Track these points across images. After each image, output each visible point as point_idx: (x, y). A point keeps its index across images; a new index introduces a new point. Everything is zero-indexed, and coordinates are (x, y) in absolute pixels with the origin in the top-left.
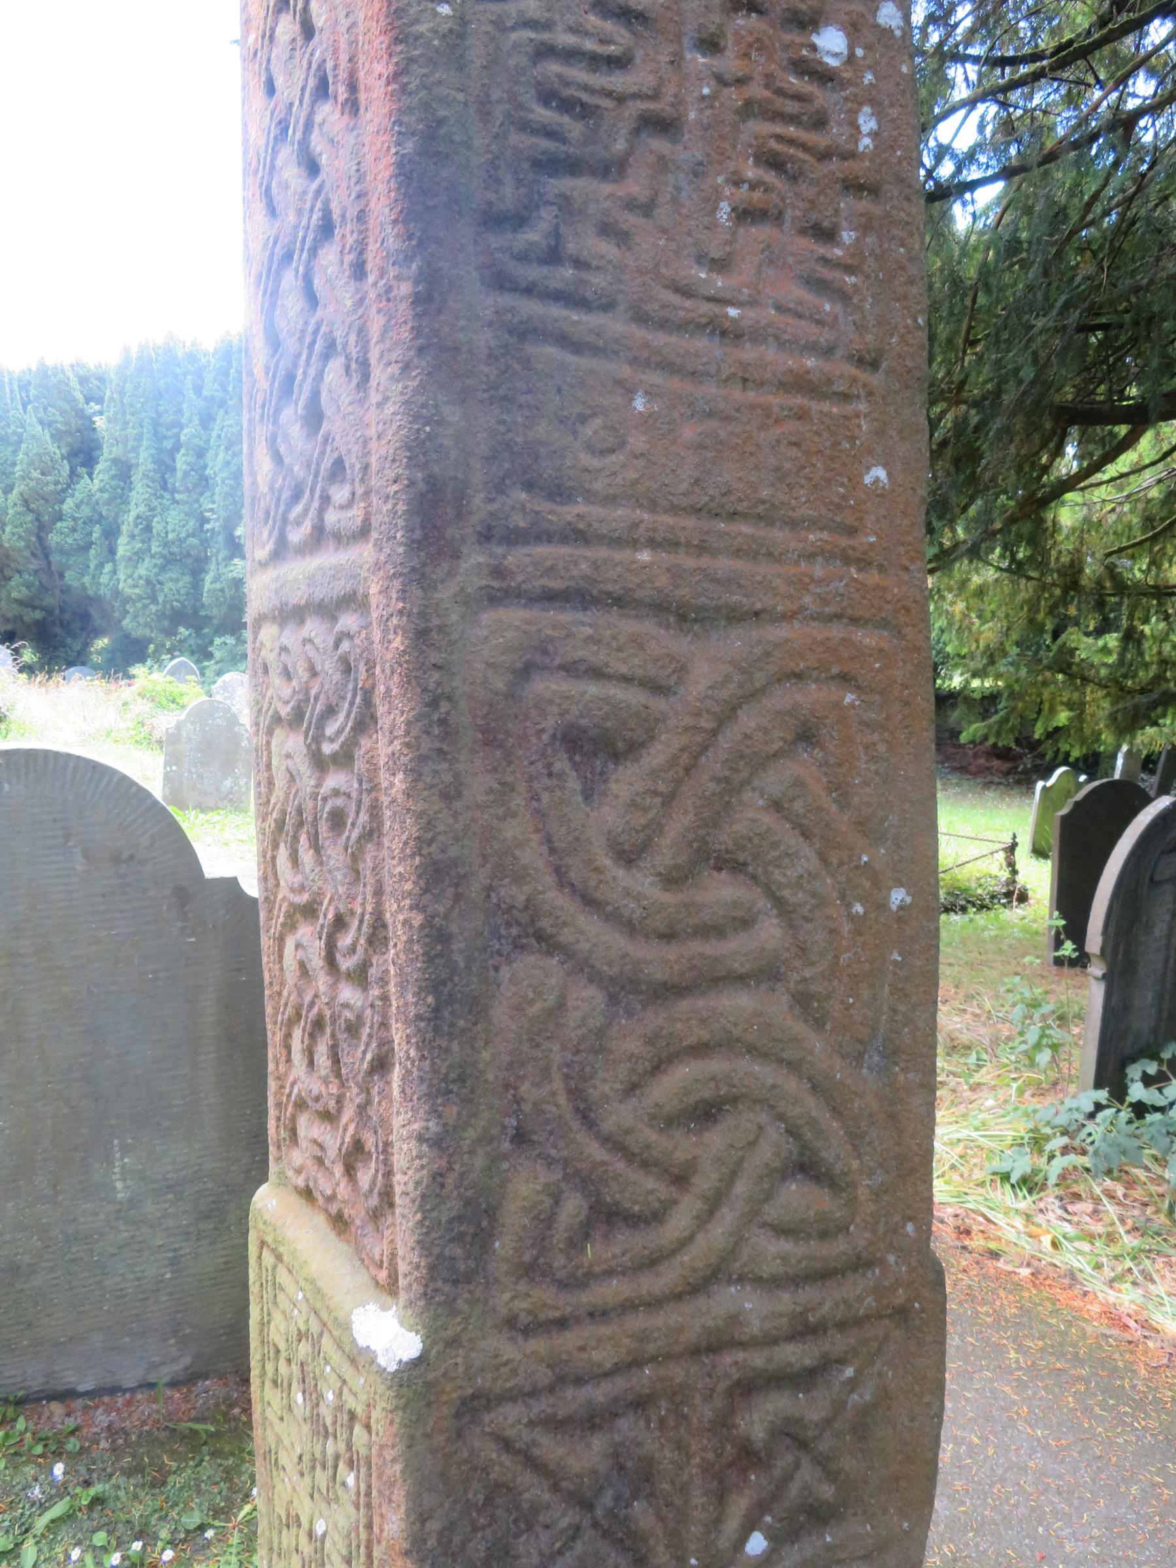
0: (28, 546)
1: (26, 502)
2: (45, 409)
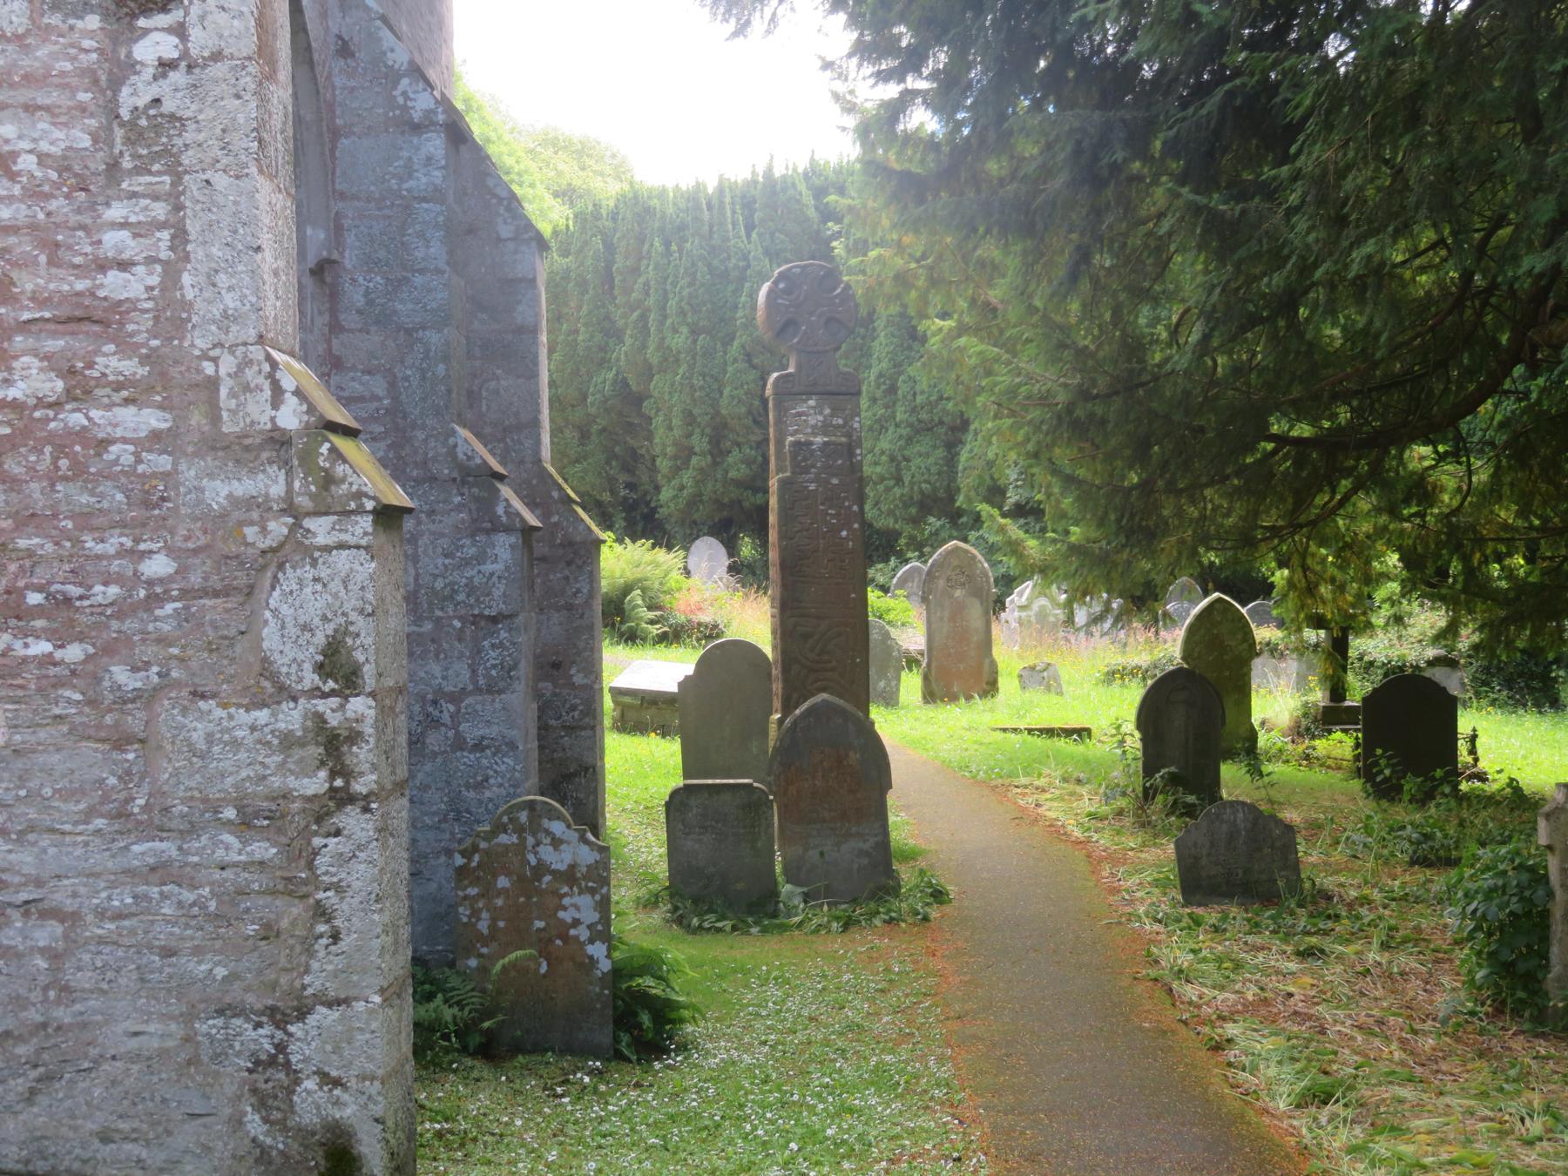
0: (749, 413)
1: (748, 357)
2: (772, 235)
